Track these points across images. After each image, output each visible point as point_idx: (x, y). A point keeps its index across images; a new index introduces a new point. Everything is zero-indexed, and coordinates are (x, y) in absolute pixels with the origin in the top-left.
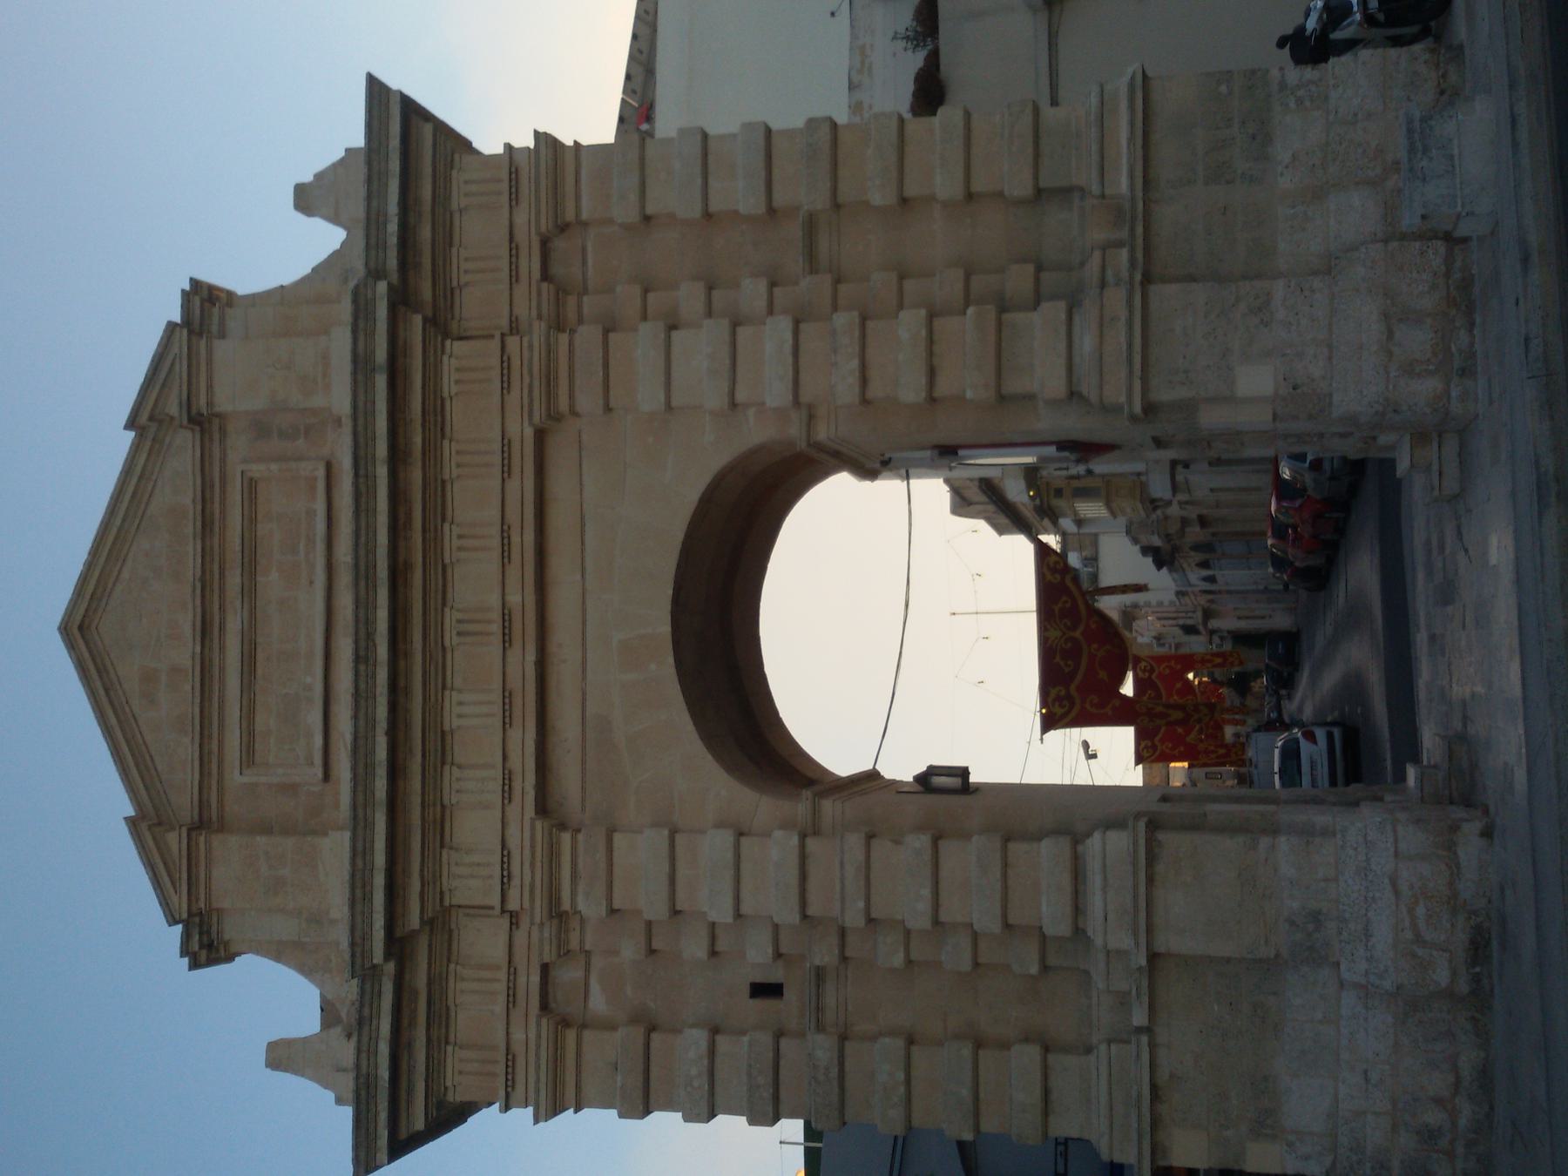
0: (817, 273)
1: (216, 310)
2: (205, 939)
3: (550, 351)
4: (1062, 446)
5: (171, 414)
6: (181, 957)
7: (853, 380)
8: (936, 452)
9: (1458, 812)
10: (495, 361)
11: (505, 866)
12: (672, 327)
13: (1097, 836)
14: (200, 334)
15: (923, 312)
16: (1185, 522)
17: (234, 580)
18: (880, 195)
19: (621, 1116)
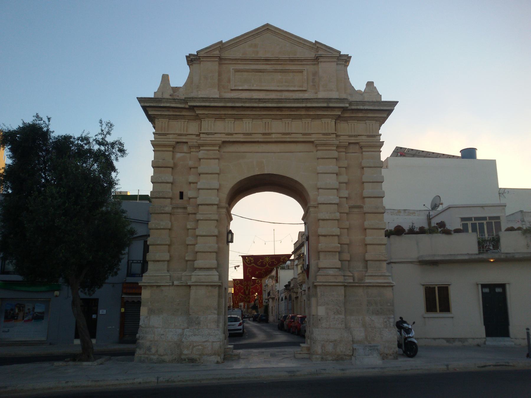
0: (349, 208)
1: (343, 63)
2: (194, 60)
3: (332, 145)
4: (308, 266)
5: (319, 52)
6: (189, 54)
7: (323, 217)
8: (307, 236)
9: (222, 357)
10: (330, 132)
11: (211, 134)
12: (337, 175)
13: (218, 273)
14: (338, 59)
15: (339, 234)
16: (297, 293)
17: (279, 67)
18: (367, 224)
19: (152, 161)
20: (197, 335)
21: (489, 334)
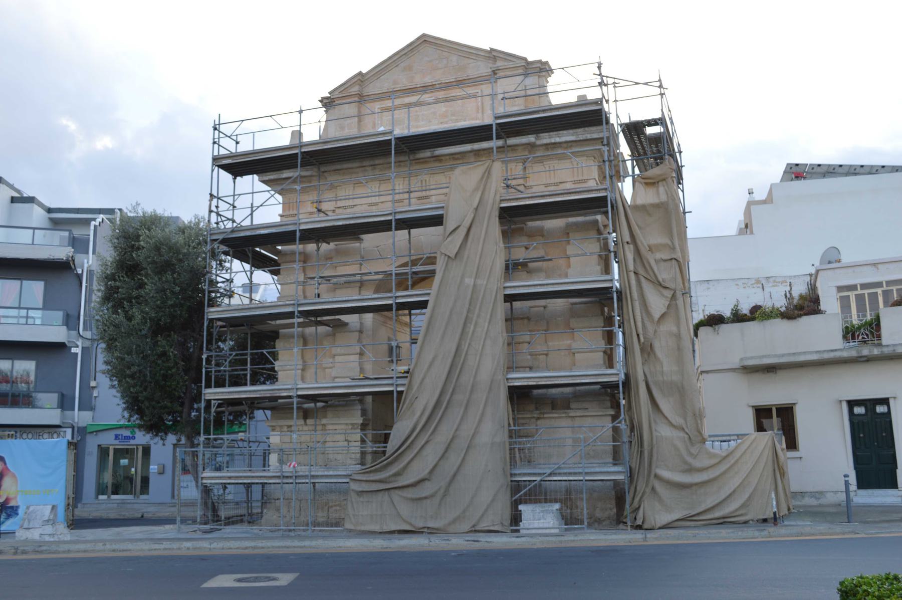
21: (863, 483)
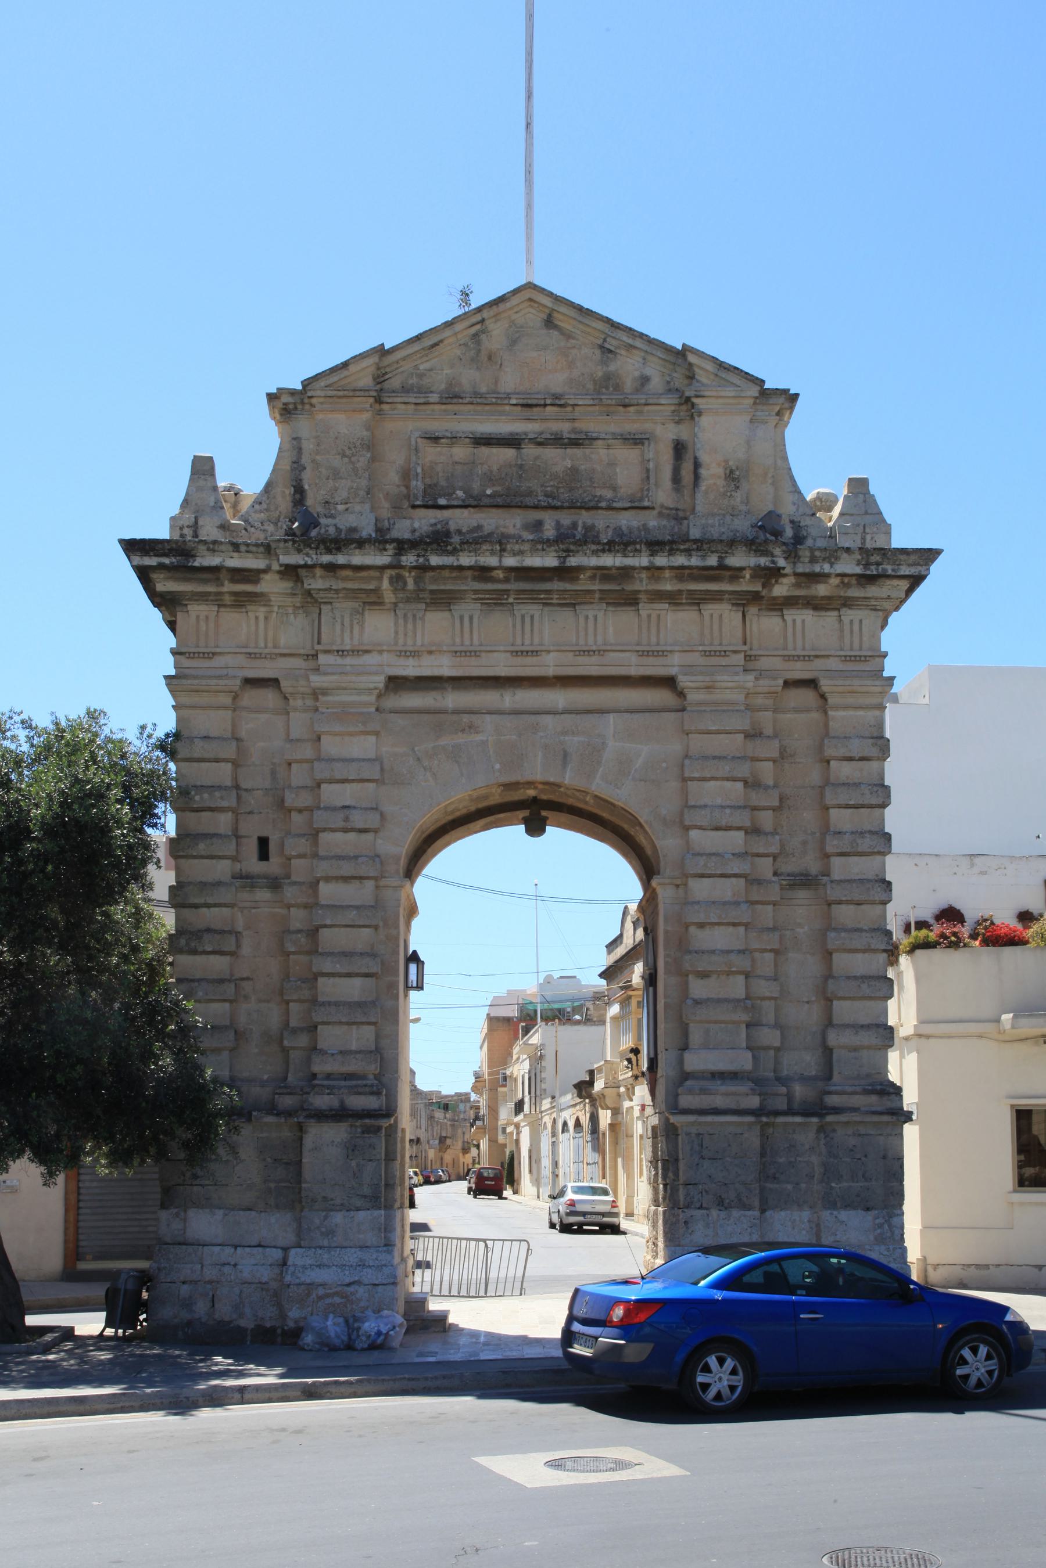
20: (329, 1267)
